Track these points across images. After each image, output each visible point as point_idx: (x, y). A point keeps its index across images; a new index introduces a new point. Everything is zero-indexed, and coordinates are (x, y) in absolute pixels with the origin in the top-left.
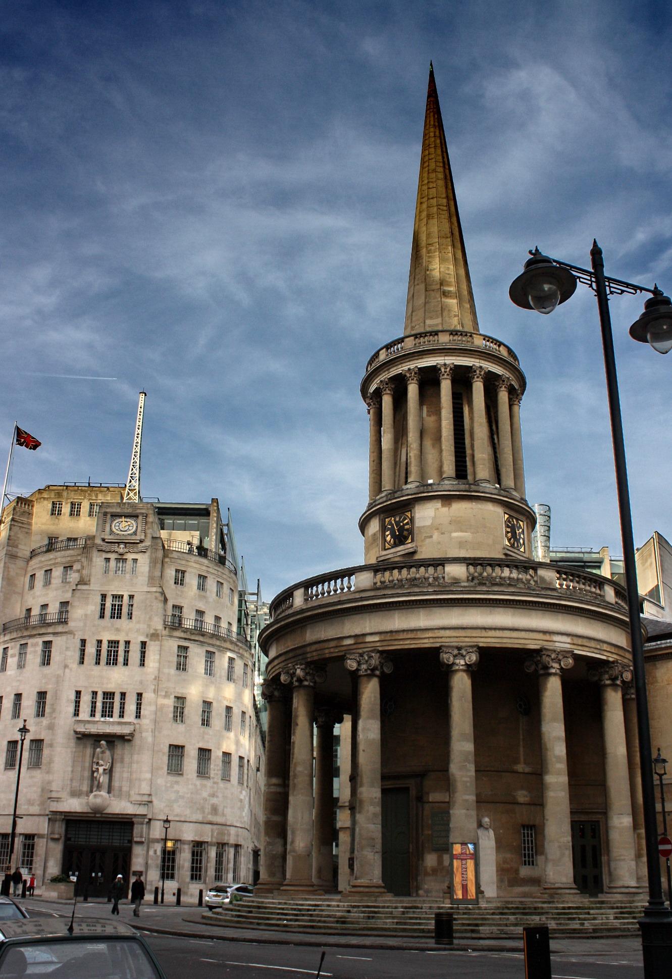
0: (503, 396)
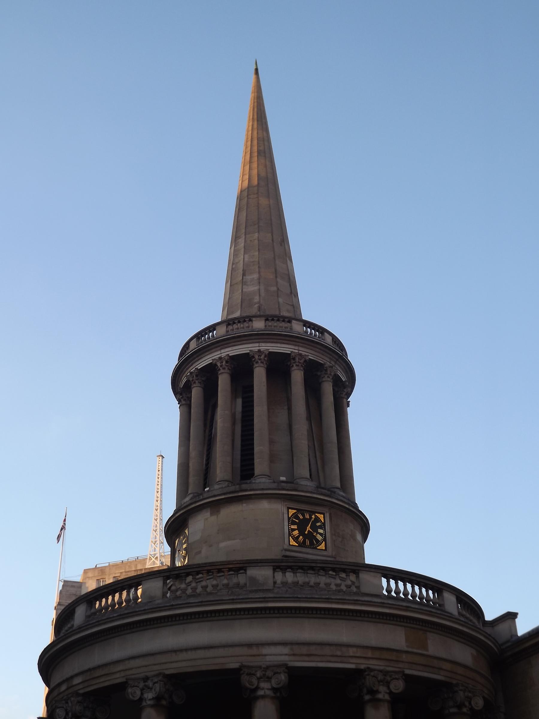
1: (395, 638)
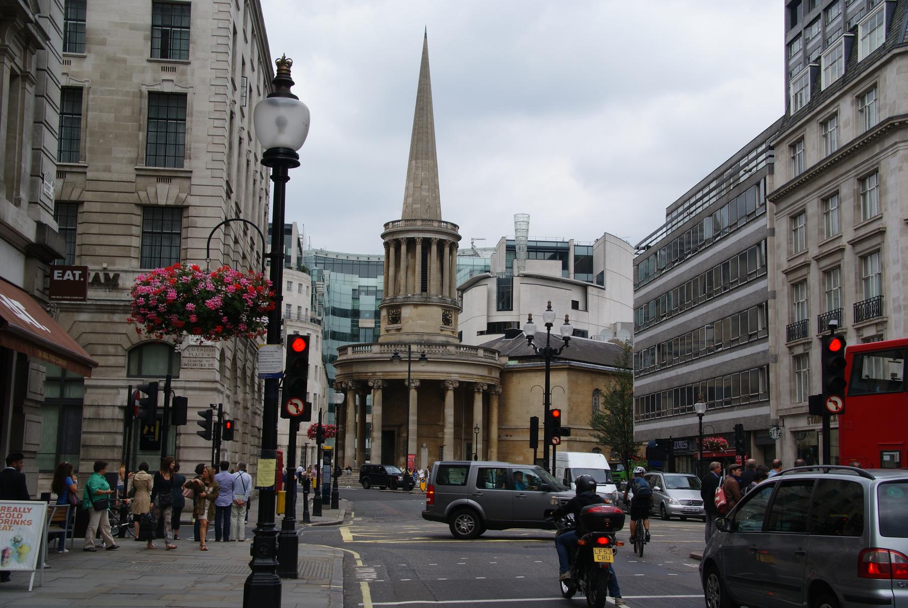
0: (447, 250)
1: (484, 372)
